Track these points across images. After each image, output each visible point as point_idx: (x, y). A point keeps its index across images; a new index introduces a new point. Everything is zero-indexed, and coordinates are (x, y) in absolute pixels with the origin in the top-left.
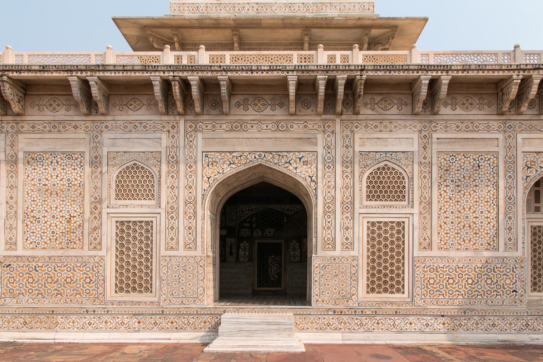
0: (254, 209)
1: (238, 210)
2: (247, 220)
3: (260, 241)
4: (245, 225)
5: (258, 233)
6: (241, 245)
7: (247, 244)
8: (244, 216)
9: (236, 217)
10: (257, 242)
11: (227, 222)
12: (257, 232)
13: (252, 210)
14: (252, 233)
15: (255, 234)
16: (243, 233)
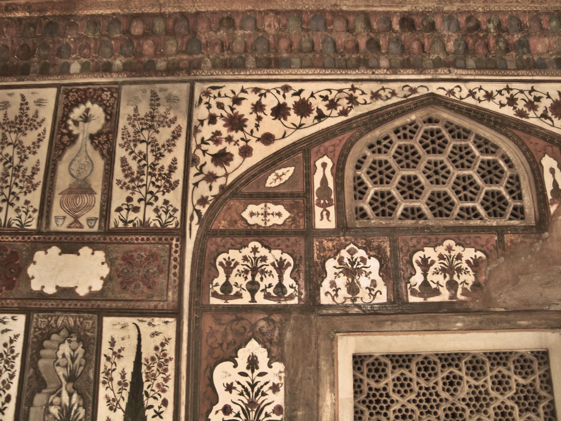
0: (318, 103)
1: (201, 112)
2: (272, 182)
3: (381, 344)
4: (254, 214)
5: (354, 278)
6: (224, 373)
7: (275, 373)
8: (246, 152)
9: (190, 160)
10: (347, 346)
11: (119, 197)
12: (352, 271)
13: (303, 108)
14: (313, 276)
15: (333, 289)
16: (239, 281)
